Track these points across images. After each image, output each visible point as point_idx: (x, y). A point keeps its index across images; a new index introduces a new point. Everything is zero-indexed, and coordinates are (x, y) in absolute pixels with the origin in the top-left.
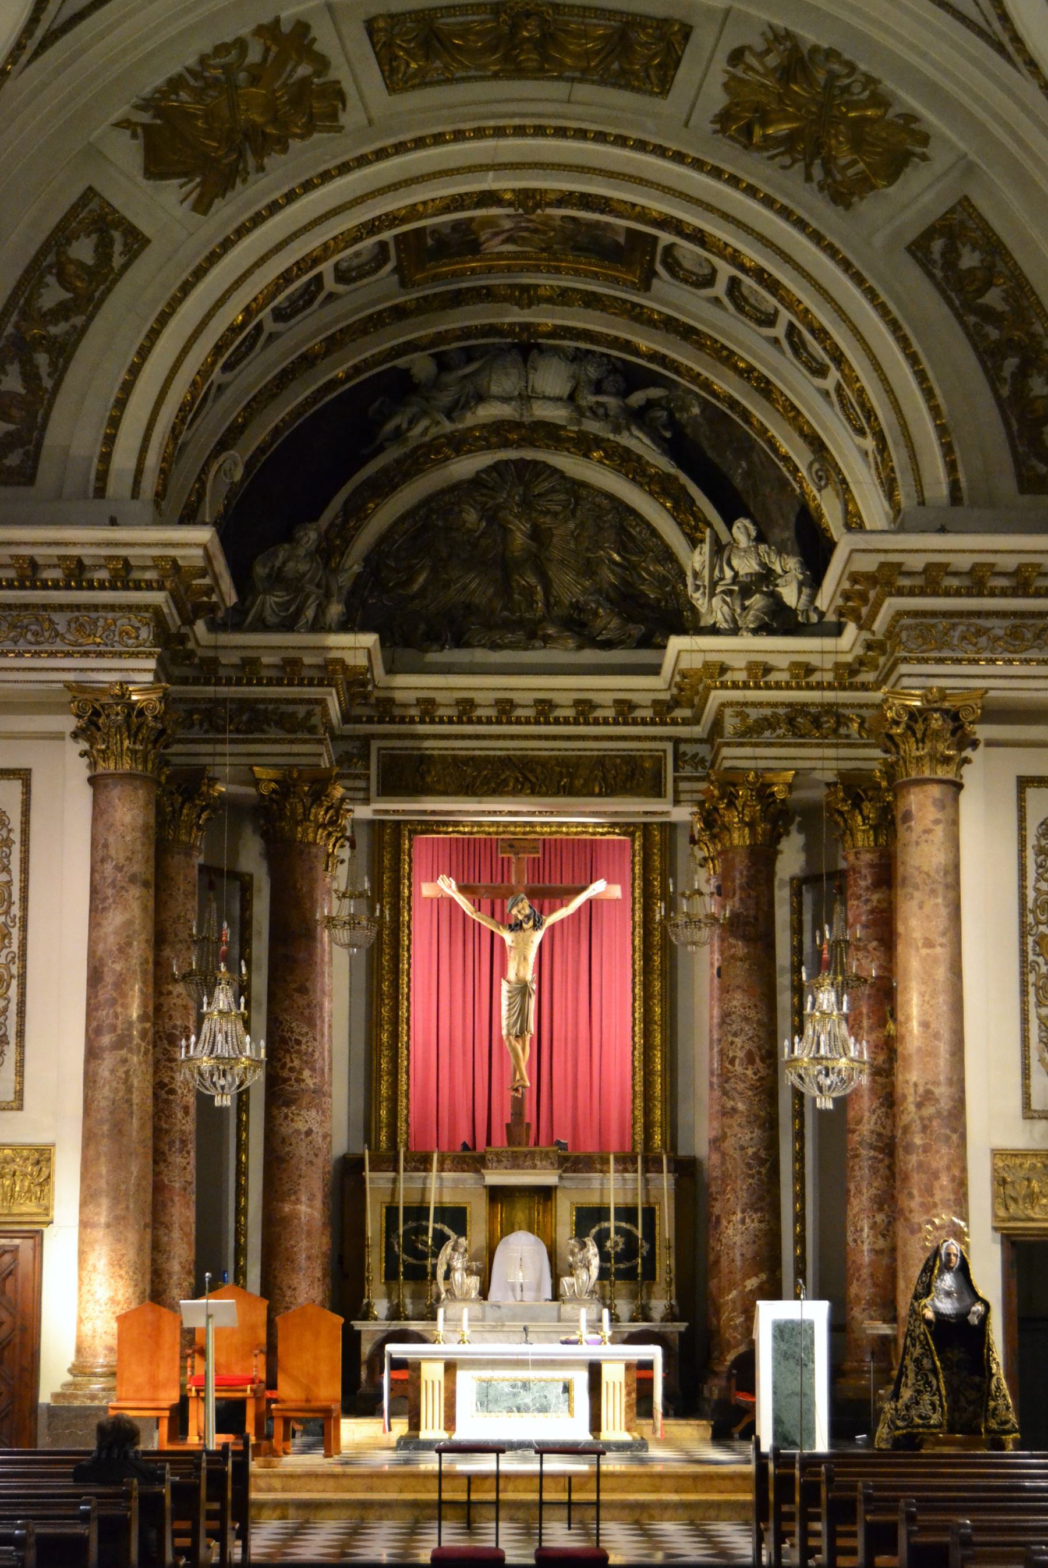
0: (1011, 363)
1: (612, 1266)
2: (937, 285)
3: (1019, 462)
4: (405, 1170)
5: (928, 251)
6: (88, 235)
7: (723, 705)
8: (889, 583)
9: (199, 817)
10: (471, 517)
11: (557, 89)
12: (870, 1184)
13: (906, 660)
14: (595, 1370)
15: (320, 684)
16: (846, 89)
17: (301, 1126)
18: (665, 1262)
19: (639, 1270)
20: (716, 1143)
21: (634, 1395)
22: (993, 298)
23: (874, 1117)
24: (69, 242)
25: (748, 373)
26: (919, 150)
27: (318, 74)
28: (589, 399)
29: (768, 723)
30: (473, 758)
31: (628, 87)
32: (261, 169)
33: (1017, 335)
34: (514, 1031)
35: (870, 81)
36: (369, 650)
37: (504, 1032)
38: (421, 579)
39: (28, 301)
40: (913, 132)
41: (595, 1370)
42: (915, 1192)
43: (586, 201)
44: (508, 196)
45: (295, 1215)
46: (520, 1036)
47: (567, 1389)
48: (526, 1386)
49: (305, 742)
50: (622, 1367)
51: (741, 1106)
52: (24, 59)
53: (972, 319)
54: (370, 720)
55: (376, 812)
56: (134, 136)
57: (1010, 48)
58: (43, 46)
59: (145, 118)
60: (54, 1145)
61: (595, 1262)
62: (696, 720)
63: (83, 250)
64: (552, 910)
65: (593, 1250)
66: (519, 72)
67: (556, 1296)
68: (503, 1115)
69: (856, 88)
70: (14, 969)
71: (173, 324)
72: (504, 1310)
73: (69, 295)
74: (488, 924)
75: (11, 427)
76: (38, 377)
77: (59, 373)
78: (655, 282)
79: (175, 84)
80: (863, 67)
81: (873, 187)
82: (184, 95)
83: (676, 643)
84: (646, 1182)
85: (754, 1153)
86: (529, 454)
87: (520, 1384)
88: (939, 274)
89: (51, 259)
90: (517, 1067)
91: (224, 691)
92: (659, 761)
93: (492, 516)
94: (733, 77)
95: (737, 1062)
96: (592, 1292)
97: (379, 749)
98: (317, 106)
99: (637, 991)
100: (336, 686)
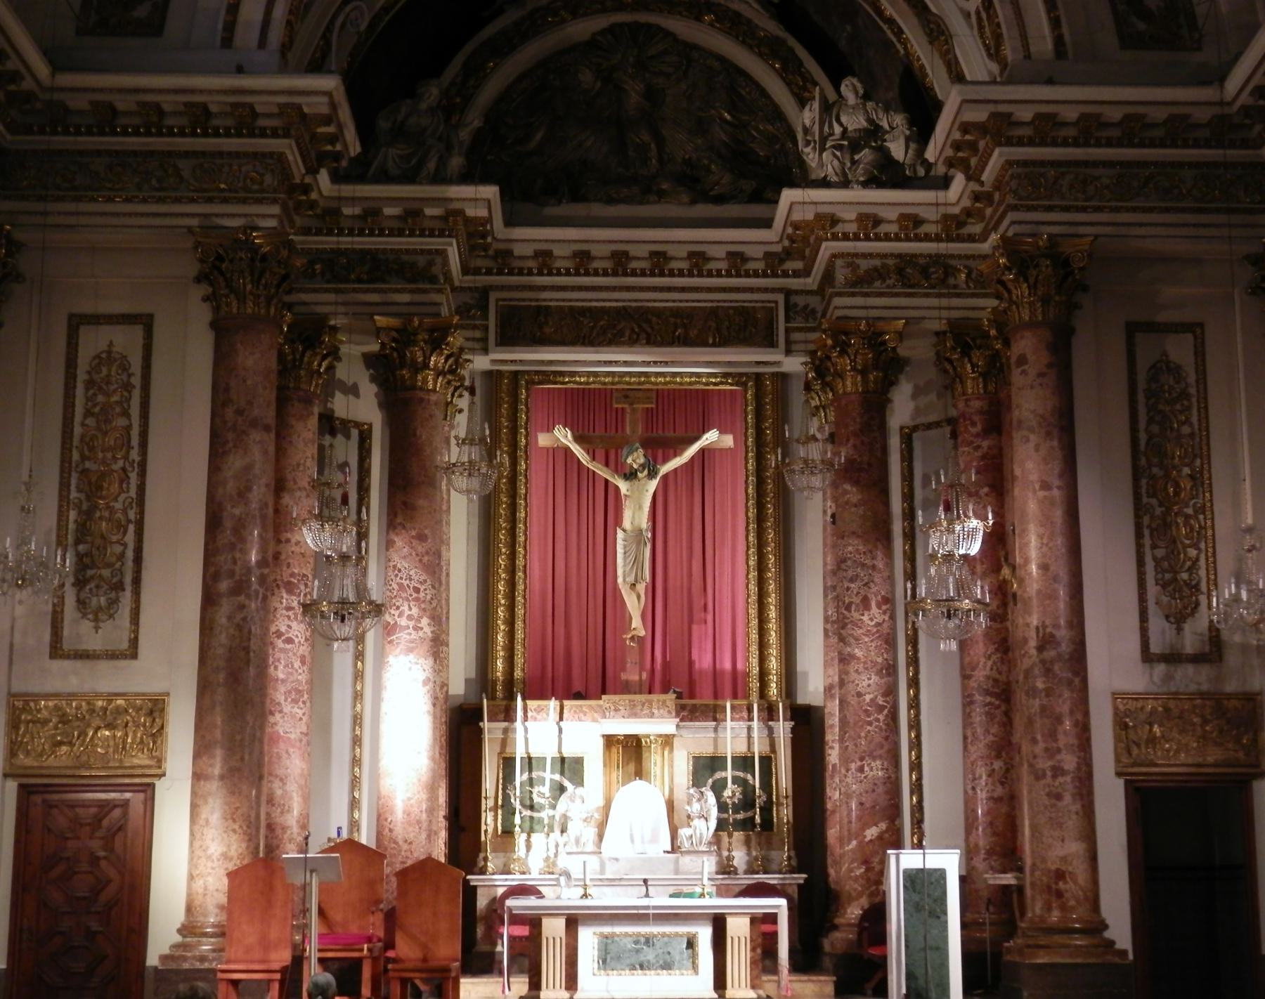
7: (834, 256)
14: (719, 923)
21: (759, 951)
29: (878, 274)
38: (539, 136)
41: (719, 923)
47: (691, 944)
48: (649, 940)
50: (747, 920)
60: (168, 694)
64: (666, 460)
67: (675, 849)
70: (132, 515)
74: (603, 472)
87: (643, 940)
91: (346, 242)
92: (771, 313)
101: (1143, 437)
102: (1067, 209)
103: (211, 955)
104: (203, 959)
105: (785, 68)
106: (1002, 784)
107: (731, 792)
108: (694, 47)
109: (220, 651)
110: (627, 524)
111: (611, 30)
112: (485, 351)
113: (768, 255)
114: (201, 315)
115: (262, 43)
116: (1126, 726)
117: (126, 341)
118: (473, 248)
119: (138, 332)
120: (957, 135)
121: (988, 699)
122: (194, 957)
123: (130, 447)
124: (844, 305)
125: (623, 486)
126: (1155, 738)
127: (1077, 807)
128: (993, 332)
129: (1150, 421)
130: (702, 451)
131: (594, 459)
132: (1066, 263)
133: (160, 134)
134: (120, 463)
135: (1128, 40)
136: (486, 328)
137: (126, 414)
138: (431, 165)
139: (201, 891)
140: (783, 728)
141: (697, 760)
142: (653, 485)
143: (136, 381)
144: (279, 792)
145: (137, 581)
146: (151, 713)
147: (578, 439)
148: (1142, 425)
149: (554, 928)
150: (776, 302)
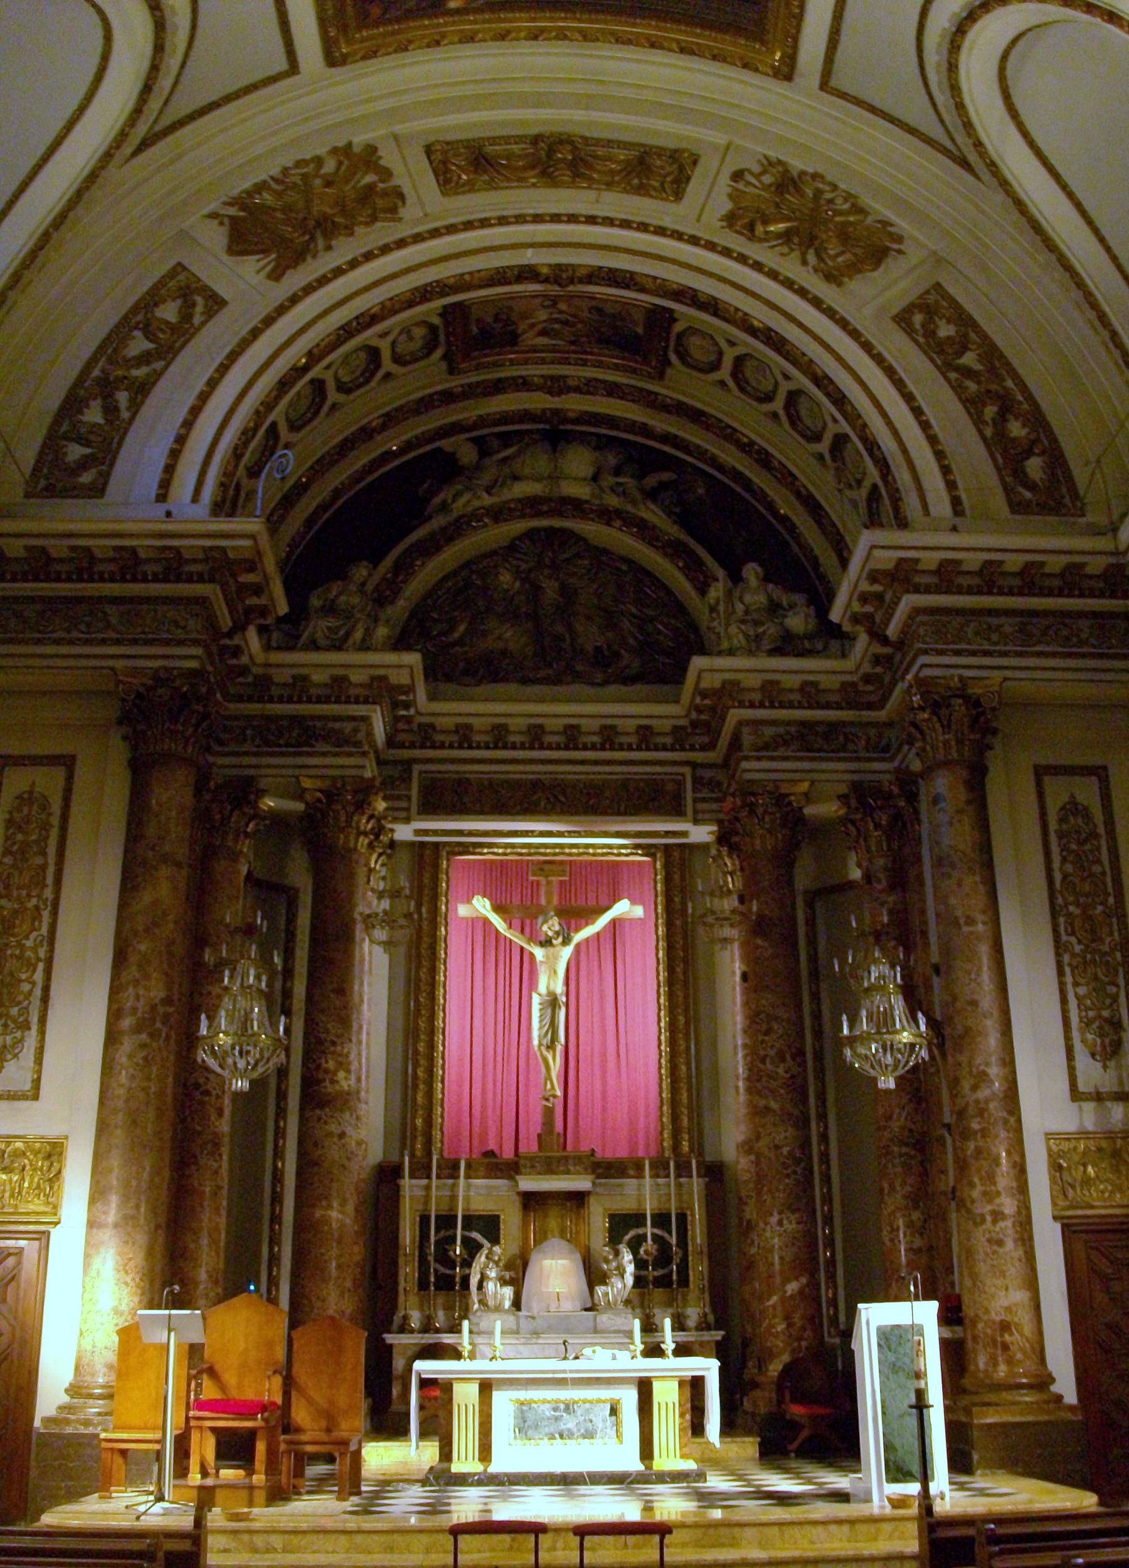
0: (990, 411)
1: (652, 1273)
3: (1008, 490)
4: (438, 1177)
6: (174, 300)
8: (907, 580)
9: (247, 825)
12: (904, 1183)
13: (925, 652)
14: (645, 1388)
15: (366, 702)
16: (831, 201)
17: (333, 1128)
18: (699, 1269)
19: (675, 1277)
20: (748, 1147)
21: (688, 1417)
22: (969, 359)
23: (904, 1114)
24: (156, 305)
25: (747, 448)
26: (895, 246)
28: (609, 480)
30: (507, 781)
32: (329, 248)
33: (993, 387)
34: (544, 1042)
35: (848, 197)
36: (411, 668)
37: (536, 1042)
40: (891, 234)
41: (645, 1388)
42: (976, 1180)
43: (613, 278)
44: (545, 271)
45: (326, 1221)
46: (551, 1047)
47: (614, 1411)
48: (569, 1407)
49: (350, 755)
50: (675, 1384)
51: (773, 1105)
52: (128, 149)
53: (953, 375)
54: (412, 746)
55: (417, 832)
56: (221, 224)
57: (973, 157)
58: (145, 144)
59: (233, 211)
60: (66, 1138)
61: (630, 1269)
62: (711, 746)
63: (169, 312)
65: (627, 1257)
68: (532, 1126)
69: (839, 201)
70: (42, 953)
71: (242, 361)
72: (539, 1321)
73: (151, 346)
75: (88, 451)
76: (117, 409)
78: (669, 371)
79: (261, 187)
80: (842, 186)
81: (859, 271)
83: (698, 662)
84: (679, 1186)
85: (790, 1153)
86: (557, 523)
87: (562, 1406)
88: (922, 340)
89: (140, 317)
90: (549, 1077)
95: (768, 1061)
96: (627, 1302)
97: (420, 773)
98: (380, 203)
99: (662, 1001)
100: (380, 704)
101: (1058, 876)
102: (973, 653)
103: (96, 1419)
104: (87, 1423)
106: (921, 1234)
107: (649, 1247)
109: (121, 1091)
110: (542, 987)
111: (530, 534)
112: (407, 820)
113: (676, 728)
114: (118, 751)
115: (196, 498)
116: (1060, 1167)
117: (49, 782)
118: (397, 719)
119: (60, 773)
120: (856, 607)
121: (904, 1150)
122: (78, 1421)
123: (45, 886)
124: (753, 769)
125: (539, 953)
126: (1090, 1179)
127: (1020, 1252)
128: (896, 790)
129: (1064, 859)
130: (614, 923)
131: (510, 926)
132: (977, 704)
133: (91, 580)
134: (34, 901)
135: (1017, 507)
136: (409, 798)
137: (44, 854)
138: (358, 635)
139: (89, 1348)
140: (696, 1184)
141: (612, 1217)
142: (567, 952)
143: (55, 821)
144: (192, 1246)
145: (43, 1020)
146: (49, 1156)
147: (498, 908)
148: (1056, 864)
149: (466, 1395)
150: (683, 775)
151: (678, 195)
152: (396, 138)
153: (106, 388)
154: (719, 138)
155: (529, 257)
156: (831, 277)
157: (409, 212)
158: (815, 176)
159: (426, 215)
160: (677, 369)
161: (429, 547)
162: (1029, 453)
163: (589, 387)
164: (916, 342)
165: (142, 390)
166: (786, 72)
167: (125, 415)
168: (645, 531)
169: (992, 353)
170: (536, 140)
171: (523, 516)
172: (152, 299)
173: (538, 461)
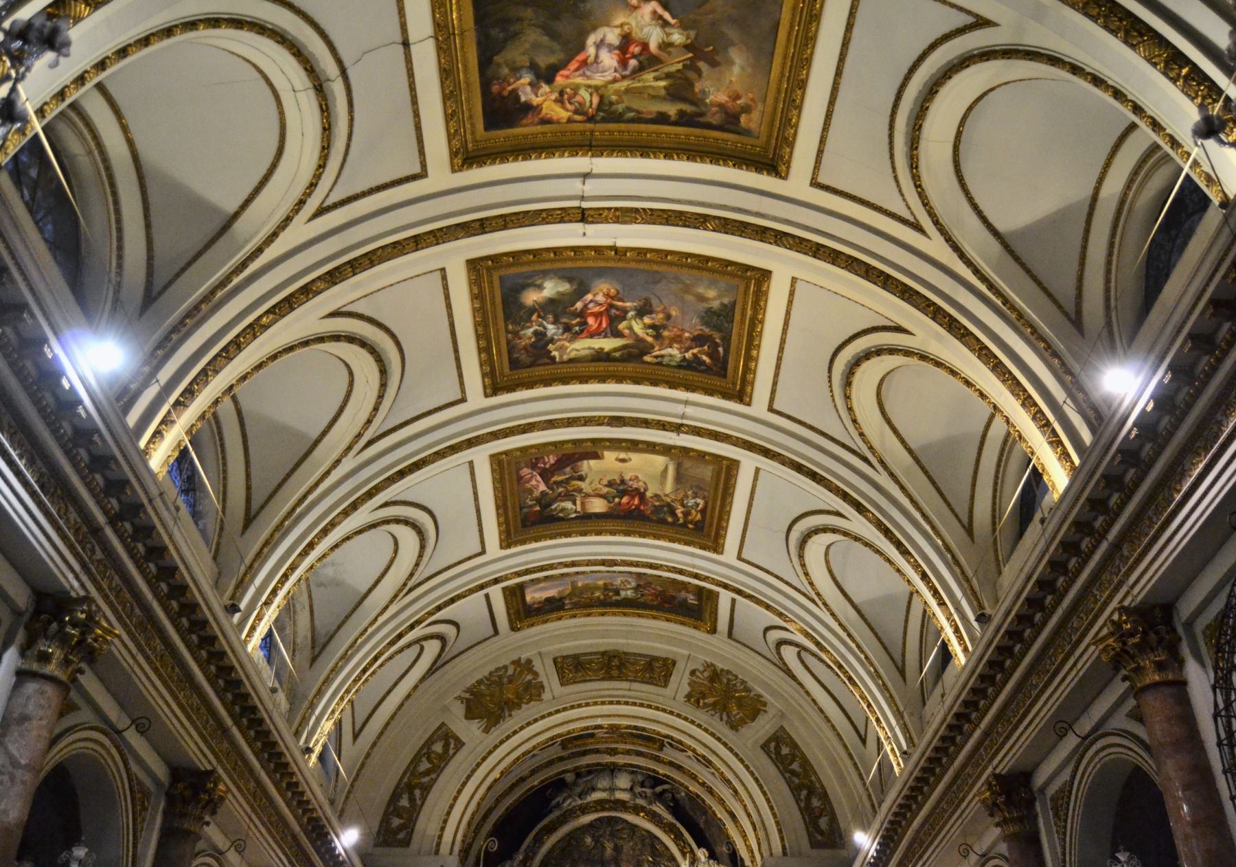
0: (804, 793)
2: (773, 761)
3: (810, 835)
5: (769, 748)
10: (589, 840)
11: (625, 685)
16: (735, 685)
22: (795, 766)
24: (433, 743)
27: (534, 679)
31: (652, 684)
32: (510, 715)
33: (806, 782)
35: (743, 682)
39: (414, 768)
53: (787, 775)
56: (462, 703)
59: (467, 695)
63: (438, 748)
66: (611, 678)
77: (424, 799)
79: (480, 682)
82: (482, 687)
88: (773, 756)
89: (425, 751)
93: (596, 840)
94: (692, 681)
98: (533, 691)
105: (676, 837)
108: (636, 826)
111: (599, 819)
135: (814, 844)
151: (666, 686)
152: (540, 654)
153: (410, 788)
154: (686, 652)
155: (599, 722)
156: (734, 727)
157: (546, 696)
158: (728, 672)
159: (554, 698)
160: (668, 749)
161: (550, 829)
162: (820, 817)
163: (628, 752)
164: (771, 757)
165: (426, 789)
166: (713, 631)
167: (419, 802)
168: (654, 818)
169: (806, 763)
170: (604, 654)
171: (597, 811)
172: (430, 742)
173: (603, 783)
